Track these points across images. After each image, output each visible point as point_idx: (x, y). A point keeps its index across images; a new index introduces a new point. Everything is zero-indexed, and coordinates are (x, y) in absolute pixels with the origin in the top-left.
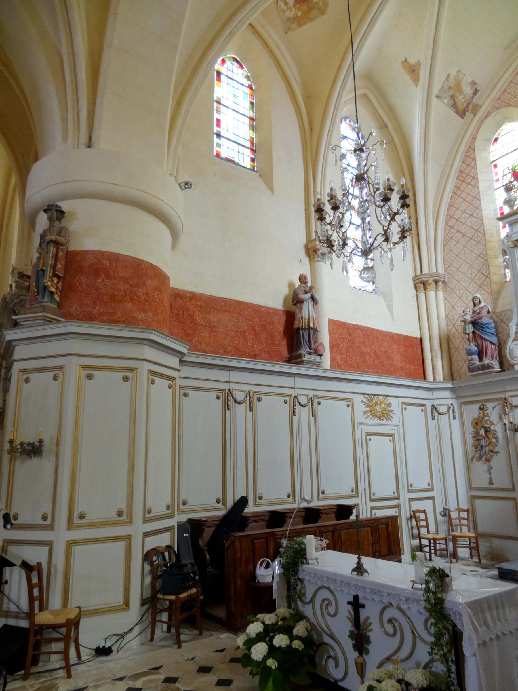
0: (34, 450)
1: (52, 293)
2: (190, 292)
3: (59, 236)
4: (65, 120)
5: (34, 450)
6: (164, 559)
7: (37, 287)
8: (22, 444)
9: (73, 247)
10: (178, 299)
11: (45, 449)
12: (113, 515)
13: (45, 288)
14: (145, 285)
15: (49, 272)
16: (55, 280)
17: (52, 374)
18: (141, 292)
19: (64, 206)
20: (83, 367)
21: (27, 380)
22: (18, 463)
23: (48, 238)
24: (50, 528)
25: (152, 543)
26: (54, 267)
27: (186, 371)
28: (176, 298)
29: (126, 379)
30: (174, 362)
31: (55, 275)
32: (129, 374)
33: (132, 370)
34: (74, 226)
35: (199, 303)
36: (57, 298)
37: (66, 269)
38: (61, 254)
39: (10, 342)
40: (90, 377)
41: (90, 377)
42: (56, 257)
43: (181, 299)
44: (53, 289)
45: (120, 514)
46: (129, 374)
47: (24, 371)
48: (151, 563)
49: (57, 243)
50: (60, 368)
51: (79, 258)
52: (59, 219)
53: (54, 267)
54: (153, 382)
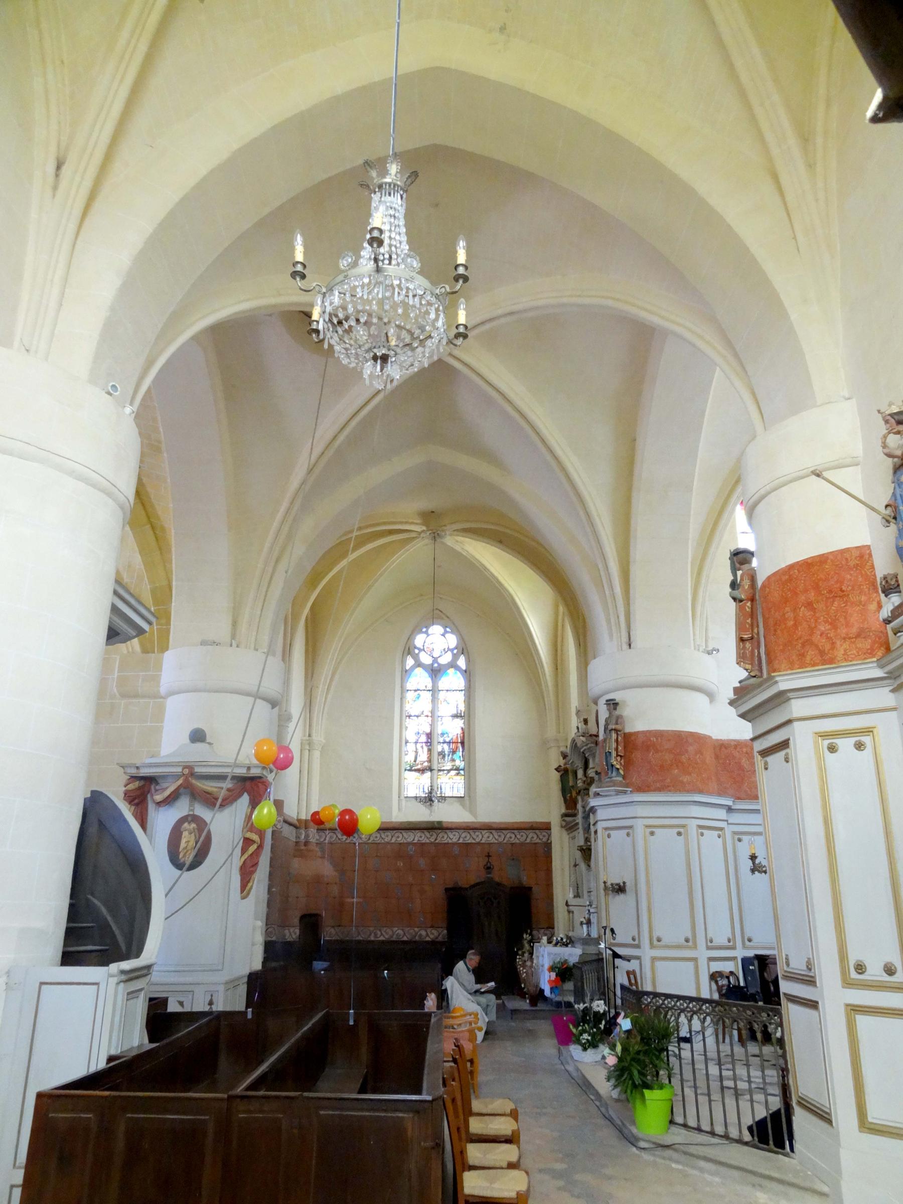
0: (620, 889)
1: (618, 769)
2: (735, 740)
3: (617, 724)
4: (608, 621)
5: (620, 889)
6: (729, 982)
7: (607, 765)
8: (612, 885)
9: (628, 730)
10: (723, 749)
11: (627, 888)
12: (682, 941)
13: (612, 766)
14: (687, 751)
15: (614, 754)
16: (619, 758)
17: (626, 831)
18: (684, 758)
19: (616, 696)
20: (647, 826)
21: (609, 836)
22: (610, 897)
23: (610, 727)
24: (638, 946)
25: (716, 967)
26: (617, 749)
27: (736, 818)
28: (720, 749)
29: (679, 834)
30: (722, 814)
31: (617, 755)
32: (682, 830)
33: (684, 826)
34: (625, 711)
35: (744, 750)
36: (622, 772)
37: (625, 747)
38: (620, 738)
39: (593, 807)
40: (652, 833)
41: (652, 833)
42: (617, 741)
43: (726, 748)
44: (618, 766)
45: (687, 940)
46: (682, 830)
47: (606, 829)
48: (717, 982)
49: (616, 731)
50: (631, 827)
51: (633, 738)
52: (615, 709)
53: (617, 749)
54: (702, 834)
